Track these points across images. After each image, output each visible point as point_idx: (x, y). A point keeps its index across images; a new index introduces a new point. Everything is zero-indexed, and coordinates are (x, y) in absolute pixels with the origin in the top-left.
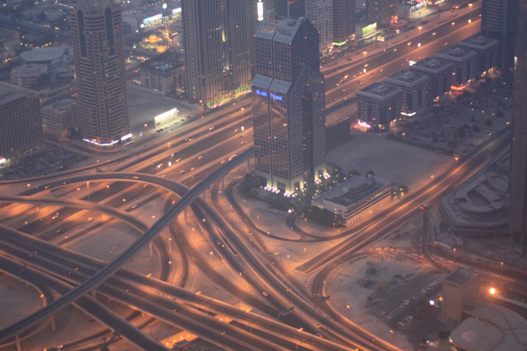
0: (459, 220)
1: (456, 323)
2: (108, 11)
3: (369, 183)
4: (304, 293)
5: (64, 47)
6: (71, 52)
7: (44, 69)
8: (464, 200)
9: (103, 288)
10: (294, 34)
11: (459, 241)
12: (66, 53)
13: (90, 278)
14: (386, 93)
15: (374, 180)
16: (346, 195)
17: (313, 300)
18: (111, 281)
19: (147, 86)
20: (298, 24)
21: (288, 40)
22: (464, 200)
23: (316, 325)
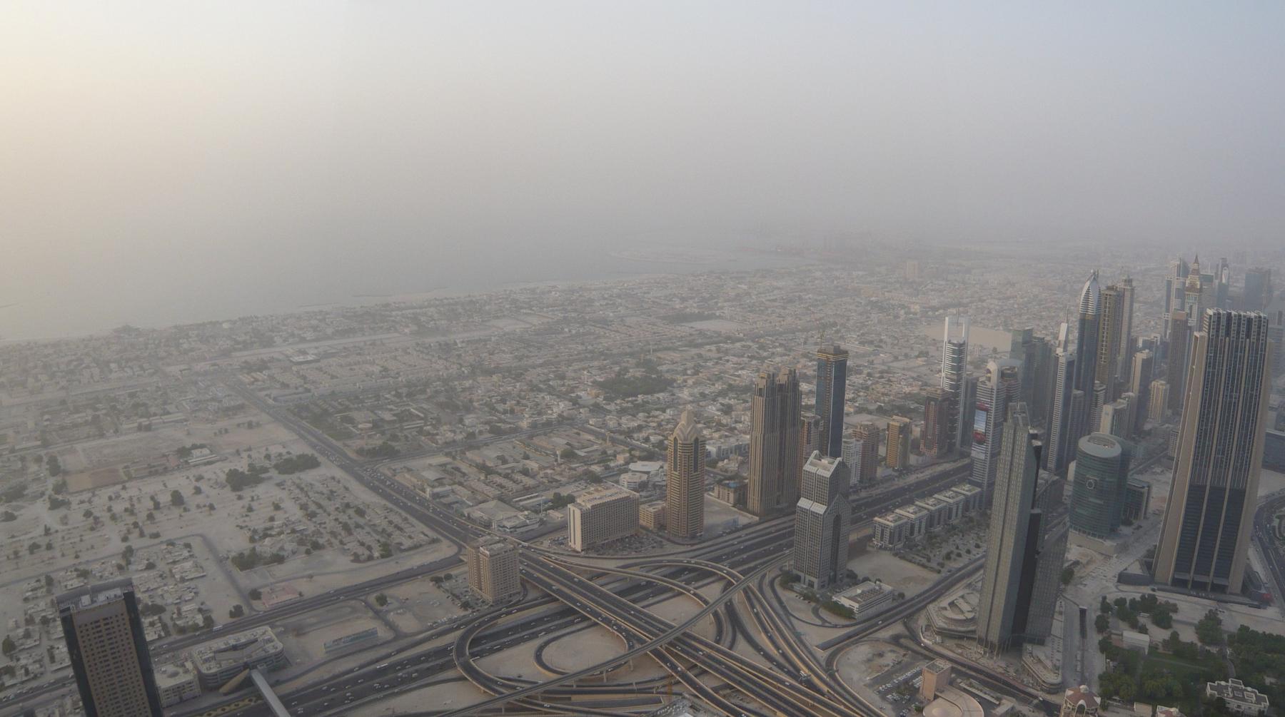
0: (940, 623)
1: (929, 702)
2: (697, 440)
3: (877, 588)
4: (821, 665)
5: (660, 463)
6: (666, 467)
7: (645, 477)
8: (945, 609)
9: (670, 644)
10: (832, 470)
11: (938, 639)
12: (662, 467)
13: (662, 635)
14: (896, 521)
15: (880, 586)
16: (859, 595)
17: (826, 671)
18: (678, 639)
19: (719, 498)
20: (836, 462)
21: (828, 474)
22: (945, 609)
23: (825, 689)
